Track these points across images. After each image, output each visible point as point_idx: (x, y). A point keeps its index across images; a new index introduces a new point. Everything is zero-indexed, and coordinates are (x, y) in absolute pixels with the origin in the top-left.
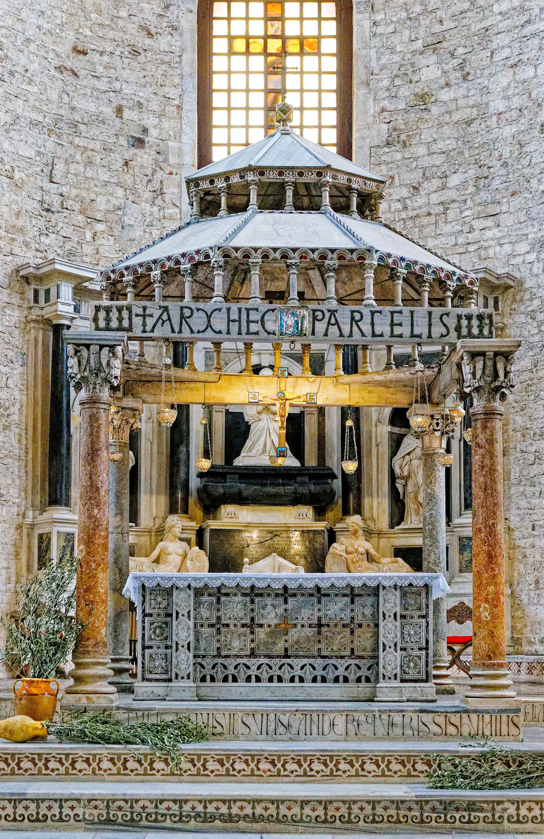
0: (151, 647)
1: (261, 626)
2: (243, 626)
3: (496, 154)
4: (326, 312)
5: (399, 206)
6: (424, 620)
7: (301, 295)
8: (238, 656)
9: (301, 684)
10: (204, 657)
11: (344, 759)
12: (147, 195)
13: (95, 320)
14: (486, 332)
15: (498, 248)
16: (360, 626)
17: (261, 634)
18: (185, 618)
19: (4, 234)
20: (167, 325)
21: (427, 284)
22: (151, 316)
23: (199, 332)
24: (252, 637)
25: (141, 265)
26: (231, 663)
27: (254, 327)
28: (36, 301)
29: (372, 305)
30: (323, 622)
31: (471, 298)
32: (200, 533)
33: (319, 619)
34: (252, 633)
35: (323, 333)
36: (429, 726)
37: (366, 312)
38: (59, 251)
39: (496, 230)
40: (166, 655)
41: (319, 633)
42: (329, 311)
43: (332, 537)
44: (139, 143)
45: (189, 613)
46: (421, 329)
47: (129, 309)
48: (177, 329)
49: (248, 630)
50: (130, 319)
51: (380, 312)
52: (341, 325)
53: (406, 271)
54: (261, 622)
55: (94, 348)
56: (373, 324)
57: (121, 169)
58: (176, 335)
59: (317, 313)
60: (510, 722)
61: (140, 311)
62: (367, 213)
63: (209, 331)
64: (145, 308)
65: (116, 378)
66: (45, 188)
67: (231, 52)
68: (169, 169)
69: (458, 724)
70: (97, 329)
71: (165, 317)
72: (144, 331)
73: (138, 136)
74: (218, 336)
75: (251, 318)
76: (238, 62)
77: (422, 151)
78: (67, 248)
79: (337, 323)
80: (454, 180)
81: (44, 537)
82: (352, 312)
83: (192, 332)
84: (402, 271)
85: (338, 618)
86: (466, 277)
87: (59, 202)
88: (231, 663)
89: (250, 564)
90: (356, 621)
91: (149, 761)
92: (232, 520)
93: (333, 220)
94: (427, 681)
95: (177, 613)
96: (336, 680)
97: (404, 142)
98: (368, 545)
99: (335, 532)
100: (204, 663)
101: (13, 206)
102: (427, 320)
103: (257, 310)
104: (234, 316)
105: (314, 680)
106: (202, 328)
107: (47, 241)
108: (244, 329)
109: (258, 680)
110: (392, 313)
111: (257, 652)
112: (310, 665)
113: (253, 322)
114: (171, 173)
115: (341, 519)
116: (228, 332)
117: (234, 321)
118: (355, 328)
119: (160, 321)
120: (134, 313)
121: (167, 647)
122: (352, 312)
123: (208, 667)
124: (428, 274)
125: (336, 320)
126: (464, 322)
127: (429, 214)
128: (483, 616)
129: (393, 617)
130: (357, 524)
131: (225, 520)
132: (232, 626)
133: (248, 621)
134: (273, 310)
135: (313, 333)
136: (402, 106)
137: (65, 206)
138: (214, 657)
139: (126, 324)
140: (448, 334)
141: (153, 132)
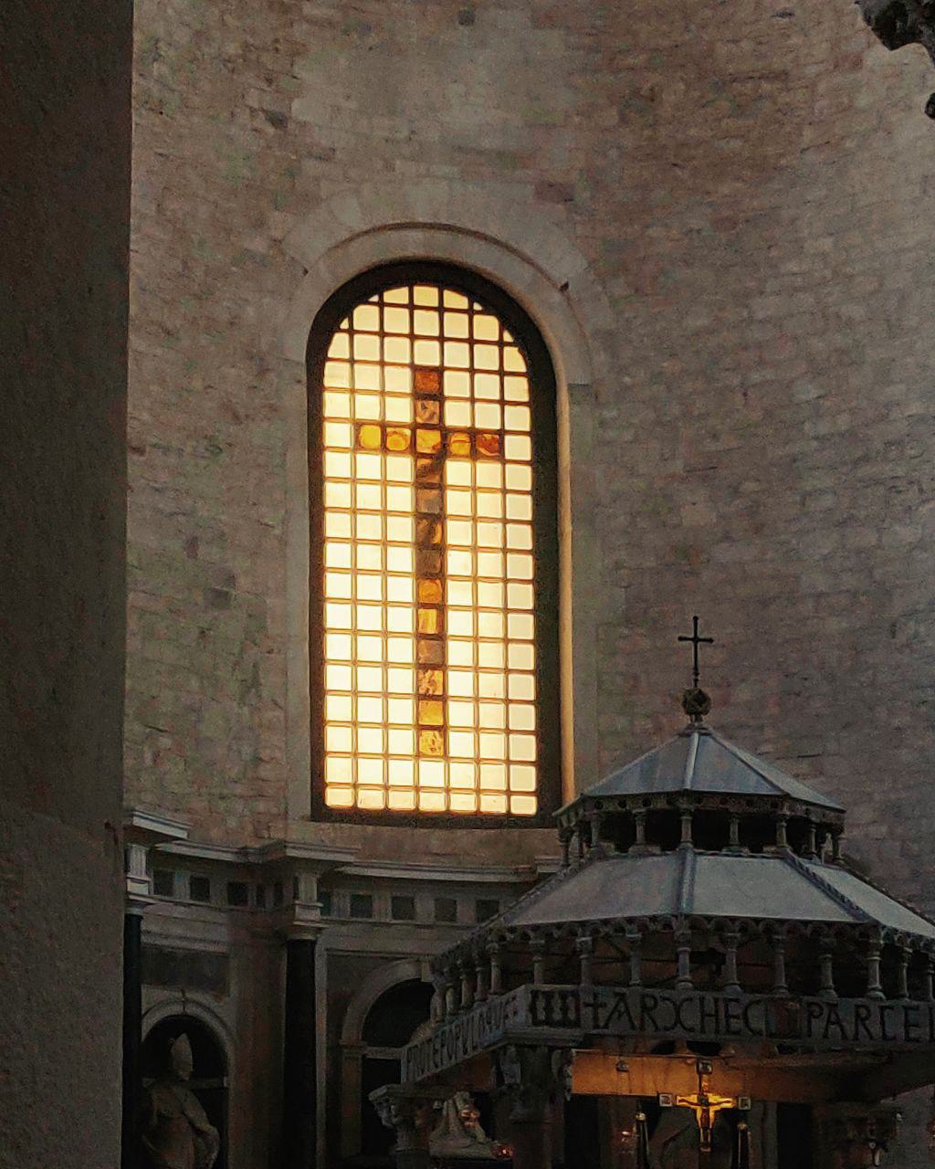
13: (532, 1009)
22: (604, 1005)
23: (666, 1029)
25: (559, 926)
27: (736, 1024)
44: (220, 599)
47: (575, 994)
48: (637, 1023)
50: (577, 1010)
51: (891, 1008)
56: (883, 1023)
61: (591, 1000)
63: (679, 1029)
67: (358, 446)
70: (536, 1022)
72: (597, 1027)
76: (369, 465)
79: (838, 1022)
83: (657, 1028)
93: (793, 864)
97: (655, 622)
103: (736, 1000)
104: (710, 1008)
108: (722, 1028)
113: (735, 1017)
116: (703, 1031)
118: (861, 1029)
120: (582, 1001)
122: (858, 1007)
134: (758, 1002)
136: (650, 562)
139: (572, 1016)
141: (244, 582)
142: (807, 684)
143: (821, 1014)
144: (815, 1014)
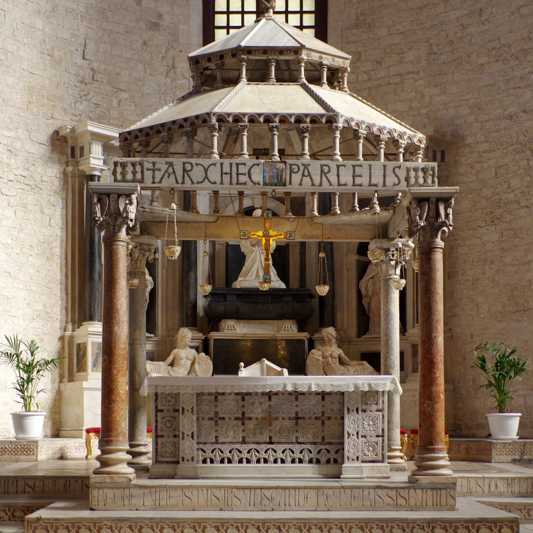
0: (163, 436)
1: (250, 419)
2: (236, 419)
3: (443, 34)
4: (300, 166)
5: (365, 77)
6: (380, 413)
7: (281, 152)
8: (232, 443)
9: (283, 465)
10: (205, 443)
11: (316, 525)
12: (163, 69)
13: (114, 173)
14: (430, 181)
15: (445, 111)
16: (329, 418)
17: (250, 425)
18: (190, 413)
19: (46, 101)
20: (172, 176)
21: (383, 143)
22: (159, 170)
24: (243, 428)
26: (226, 448)
27: (243, 179)
28: (73, 156)
29: (338, 160)
30: (300, 415)
31: (419, 154)
32: (206, 342)
33: (297, 413)
34: (243, 424)
35: (299, 183)
36: (383, 498)
37: (333, 165)
38: (91, 115)
39: (443, 96)
40: (174, 443)
41: (297, 424)
42: (303, 165)
43: (312, 346)
45: (192, 408)
46: (377, 179)
48: (180, 180)
49: (240, 422)
50: (142, 172)
51: (344, 166)
52: (313, 177)
53: (365, 132)
54: (250, 416)
55: (113, 197)
56: (338, 176)
57: (140, 48)
58: (180, 185)
59: (293, 167)
60: (448, 495)
61: (151, 166)
62: (336, 84)
64: (154, 164)
65: (131, 220)
66: (78, 63)
68: (180, 48)
69: (407, 498)
70: (116, 180)
71: (170, 170)
73: (154, 21)
74: (214, 186)
75: (240, 171)
77: (384, 32)
78: (97, 112)
79: (309, 175)
80: (410, 56)
81: (81, 346)
82: (322, 166)
83: (193, 183)
84: (363, 132)
85: (312, 412)
86: (415, 136)
87: (91, 75)
88: (226, 448)
89: (244, 368)
90: (326, 415)
91: (160, 528)
92: (231, 332)
94: (382, 462)
95: (183, 409)
96: (310, 461)
98: (340, 351)
99: (313, 341)
100: (204, 448)
101: (54, 79)
102: (383, 172)
103: (245, 164)
104: (226, 169)
105: (293, 461)
106: (201, 180)
107: (81, 107)
108: (234, 180)
109: (248, 461)
110: (354, 166)
111: (247, 440)
112: (290, 449)
114: (181, 51)
115: (319, 331)
116: (222, 183)
117: (226, 174)
118: (324, 178)
119: (167, 174)
121: (175, 436)
123: (209, 452)
124: (384, 134)
125: (309, 173)
126: (412, 174)
127: (389, 84)
128: (426, 410)
129: (355, 411)
130: (332, 335)
131: (225, 331)
132: (227, 419)
133: (240, 416)
134: (258, 165)
135: (290, 183)
137: (95, 79)
138: (213, 443)
139: (139, 176)
140: (399, 183)
141: (167, 18)
142: (440, 47)
143: (299, 171)
144: (294, 171)
